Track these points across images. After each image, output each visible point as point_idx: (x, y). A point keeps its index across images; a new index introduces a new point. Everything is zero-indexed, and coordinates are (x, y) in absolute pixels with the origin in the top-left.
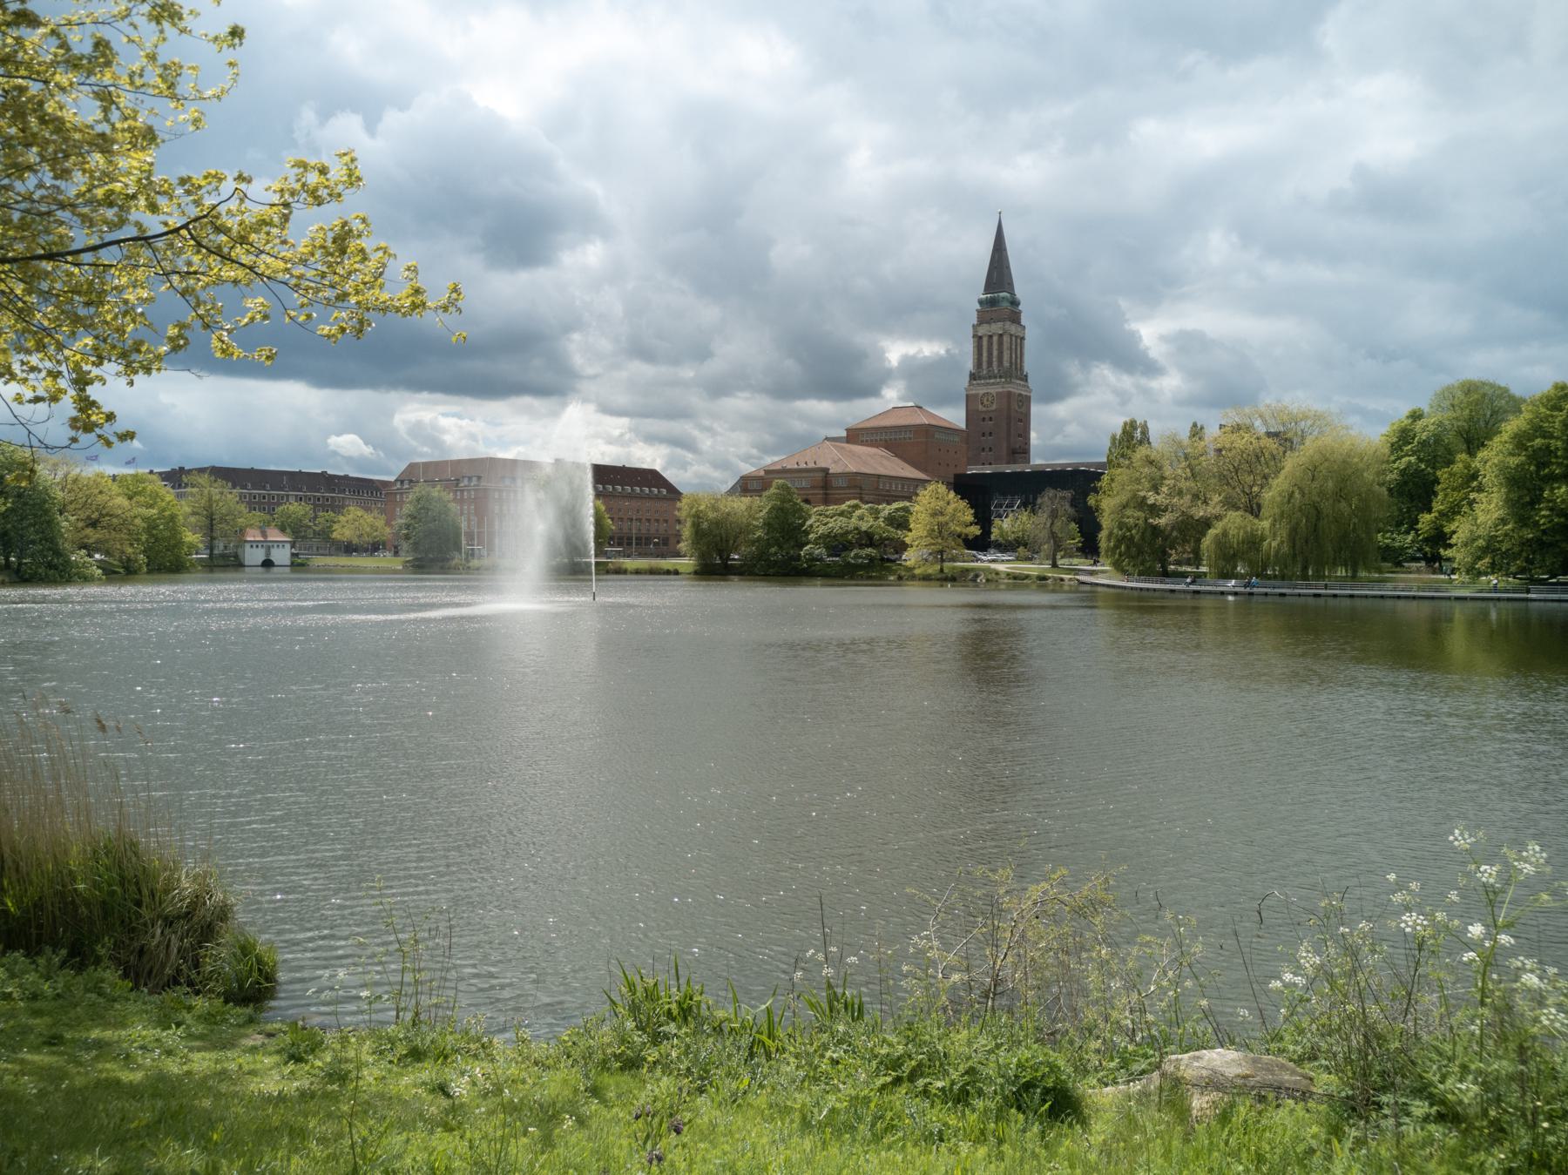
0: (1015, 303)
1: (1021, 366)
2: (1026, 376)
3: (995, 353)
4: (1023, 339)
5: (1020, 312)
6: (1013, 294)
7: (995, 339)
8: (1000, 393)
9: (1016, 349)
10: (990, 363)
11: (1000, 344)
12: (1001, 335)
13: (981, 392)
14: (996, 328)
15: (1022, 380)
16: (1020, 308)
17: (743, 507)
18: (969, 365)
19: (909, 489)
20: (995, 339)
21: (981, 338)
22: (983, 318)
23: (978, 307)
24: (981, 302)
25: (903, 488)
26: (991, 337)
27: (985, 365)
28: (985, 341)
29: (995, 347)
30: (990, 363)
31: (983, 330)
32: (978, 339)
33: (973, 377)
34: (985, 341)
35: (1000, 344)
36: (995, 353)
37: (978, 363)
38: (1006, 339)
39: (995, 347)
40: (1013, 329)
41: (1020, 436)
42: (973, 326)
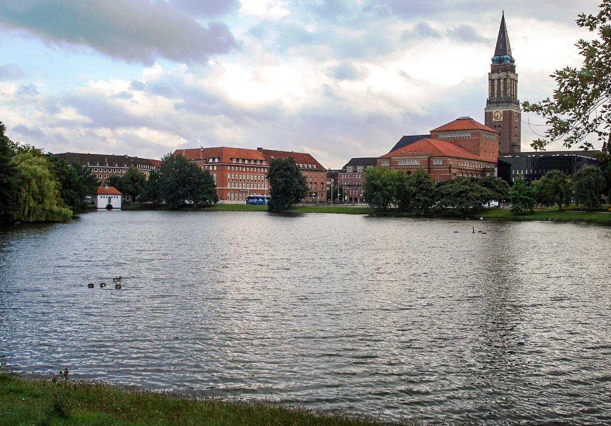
0: (512, 61)
1: (516, 96)
3: (502, 89)
4: (517, 81)
5: (515, 66)
6: (511, 57)
7: (502, 81)
9: (513, 87)
11: (505, 83)
12: (505, 79)
14: (502, 75)
15: (516, 104)
16: (515, 64)
17: (396, 173)
18: (487, 96)
19: (358, 176)
20: (502, 81)
21: (493, 80)
22: (494, 70)
23: (491, 63)
24: (493, 60)
26: (499, 80)
27: (496, 96)
28: (496, 82)
29: (502, 86)
30: (499, 94)
31: (495, 76)
32: (491, 81)
33: (489, 102)
34: (496, 82)
35: (505, 83)
36: (502, 89)
39: (502, 86)
40: (512, 75)
41: (516, 136)
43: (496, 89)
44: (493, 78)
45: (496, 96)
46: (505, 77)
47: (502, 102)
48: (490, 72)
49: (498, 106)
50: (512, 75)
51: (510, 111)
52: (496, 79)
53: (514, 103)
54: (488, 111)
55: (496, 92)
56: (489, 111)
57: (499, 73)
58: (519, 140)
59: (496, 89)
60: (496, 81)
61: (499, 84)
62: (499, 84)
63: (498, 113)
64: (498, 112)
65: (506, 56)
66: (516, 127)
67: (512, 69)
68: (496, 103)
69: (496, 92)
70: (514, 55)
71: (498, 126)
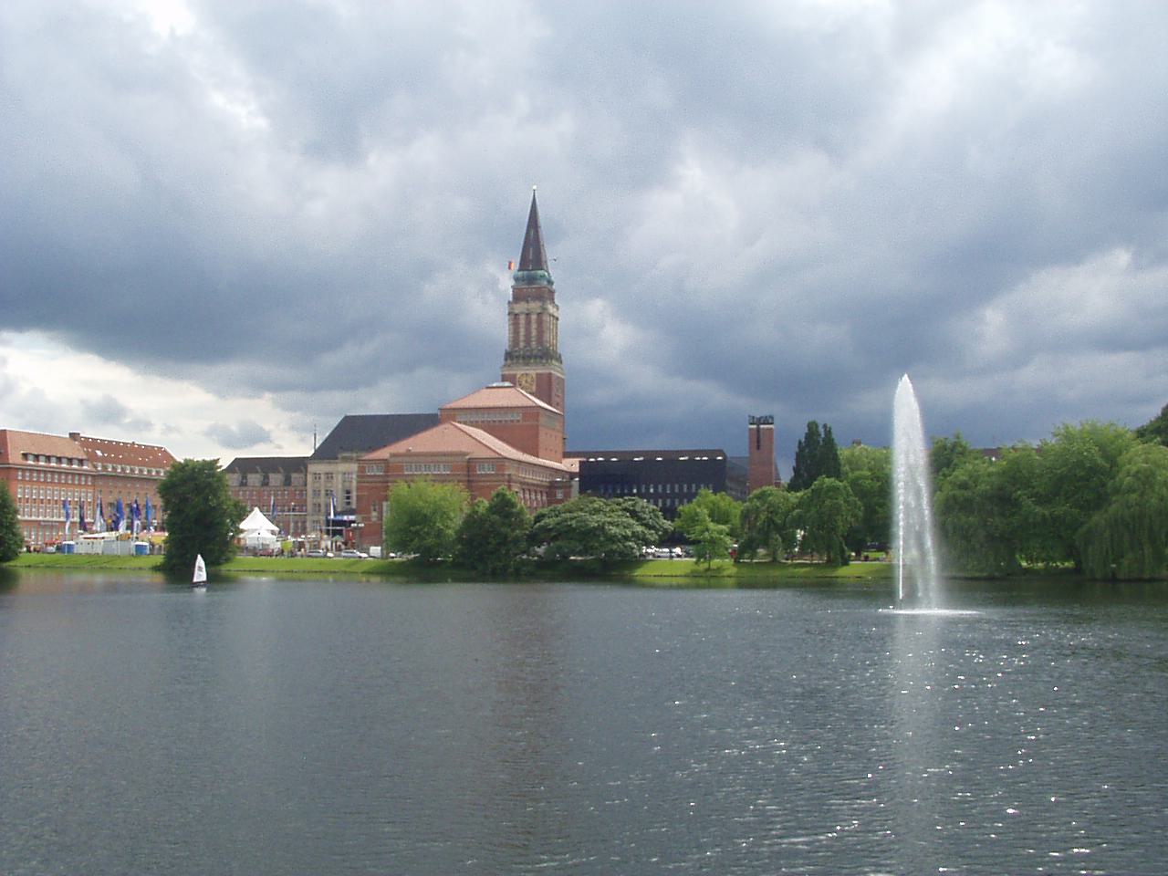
2: (560, 356)
3: (534, 333)
7: (534, 317)
8: (541, 374)
10: (528, 341)
11: (540, 322)
12: (539, 314)
16: (554, 287)
20: (534, 317)
27: (522, 345)
28: (522, 319)
29: (534, 326)
30: (528, 341)
31: (521, 307)
32: (514, 317)
34: (522, 317)
36: (534, 333)
37: (515, 341)
39: (534, 326)
42: (509, 302)
44: (516, 312)
45: (522, 345)
46: (539, 311)
47: (536, 357)
48: (511, 299)
49: (527, 364)
50: (551, 309)
51: (550, 374)
52: (522, 313)
54: (507, 373)
55: (522, 338)
56: (512, 372)
57: (528, 302)
60: (522, 317)
61: (528, 323)
62: (528, 323)
64: (527, 374)
65: (540, 272)
68: (523, 358)
69: (522, 338)
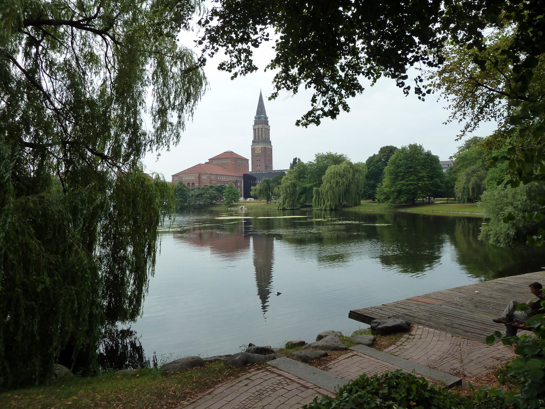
0: (266, 118)
4: (269, 130)
7: (260, 130)
13: (256, 147)
14: (260, 126)
18: (252, 138)
20: (260, 130)
22: (256, 123)
24: (255, 118)
25: (226, 178)
26: (259, 129)
27: (257, 138)
29: (260, 132)
30: (259, 137)
31: (256, 127)
32: (255, 130)
33: (253, 142)
35: (262, 131)
37: (255, 137)
38: (263, 130)
39: (260, 132)
40: (266, 127)
41: (269, 161)
43: (257, 135)
45: (257, 138)
53: (267, 142)
58: (272, 164)
59: (257, 135)
61: (259, 131)
62: (259, 131)
63: (259, 147)
66: (269, 156)
67: (266, 123)
70: (268, 115)
71: (258, 155)
